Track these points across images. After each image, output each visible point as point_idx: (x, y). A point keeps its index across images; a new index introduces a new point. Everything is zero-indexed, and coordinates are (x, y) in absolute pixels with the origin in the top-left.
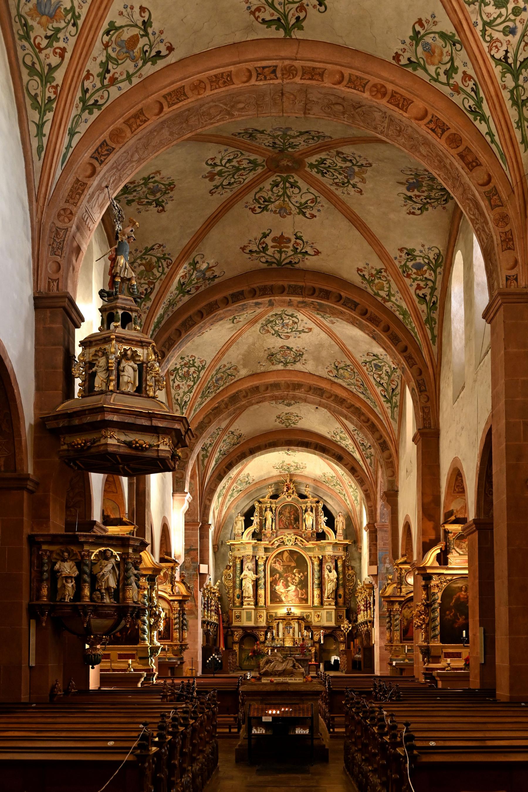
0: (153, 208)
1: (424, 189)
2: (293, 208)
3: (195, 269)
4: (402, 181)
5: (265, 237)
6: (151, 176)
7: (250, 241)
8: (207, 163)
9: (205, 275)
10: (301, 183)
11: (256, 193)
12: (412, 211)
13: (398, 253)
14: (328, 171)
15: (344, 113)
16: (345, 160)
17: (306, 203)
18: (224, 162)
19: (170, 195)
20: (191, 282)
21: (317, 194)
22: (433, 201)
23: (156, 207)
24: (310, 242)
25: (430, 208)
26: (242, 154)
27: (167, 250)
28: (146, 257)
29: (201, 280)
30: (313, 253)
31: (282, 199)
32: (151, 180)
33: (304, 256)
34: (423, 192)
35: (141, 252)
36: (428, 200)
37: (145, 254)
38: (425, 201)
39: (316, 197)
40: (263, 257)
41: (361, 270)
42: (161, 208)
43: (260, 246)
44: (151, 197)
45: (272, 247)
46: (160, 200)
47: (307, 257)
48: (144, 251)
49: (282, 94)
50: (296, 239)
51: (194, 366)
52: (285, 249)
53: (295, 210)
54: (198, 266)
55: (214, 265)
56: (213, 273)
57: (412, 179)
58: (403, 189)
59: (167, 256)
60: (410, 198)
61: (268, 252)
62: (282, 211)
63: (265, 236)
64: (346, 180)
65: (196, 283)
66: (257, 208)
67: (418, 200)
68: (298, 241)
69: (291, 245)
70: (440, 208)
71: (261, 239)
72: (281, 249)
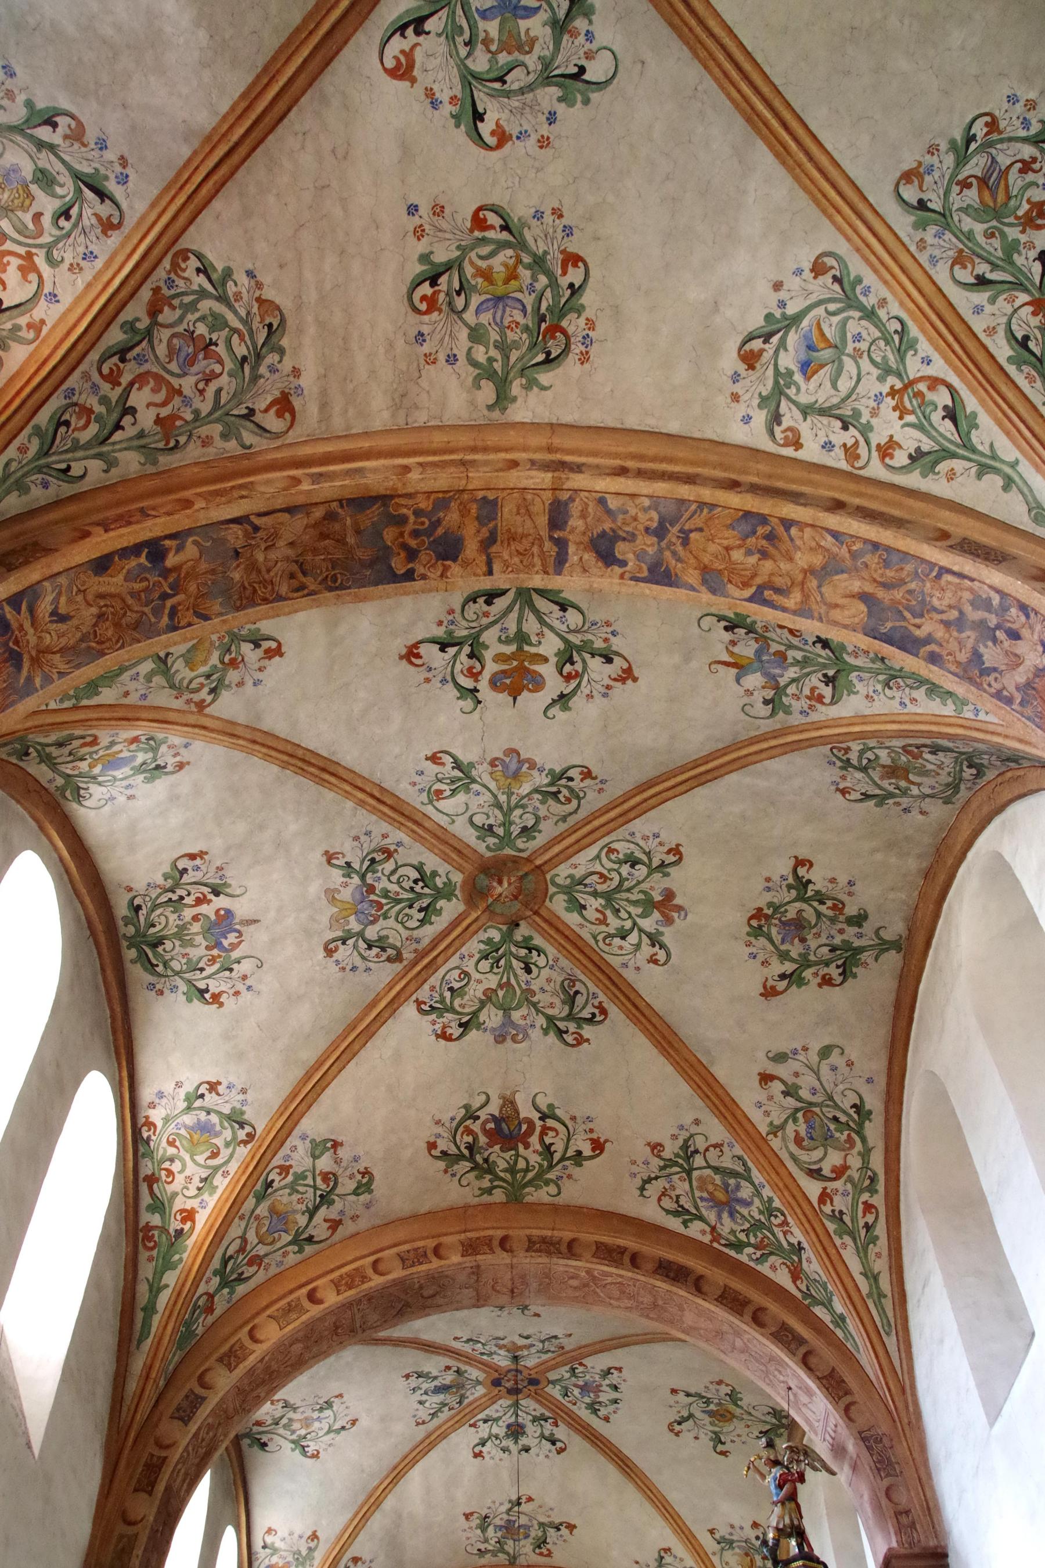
0: (818, 877)
1: (196, 928)
2: (486, 779)
3: (780, 690)
4: (252, 927)
5: (562, 696)
6: (785, 982)
7: (605, 695)
8: (668, 955)
9: (759, 653)
10: (470, 836)
11: (576, 811)
12: (198, 862)
13: (185, 755)
14: (412, 888)
15: (421, 1287)
16: (380, 944)
17: (454, 792)
18: (633, 938)
19: (768, 897)
20: (805, 662)
21: (429, 810)
22: (164, 899)
23: (809, 882)
24: (436, 682)
25: (160, 880)
26: (595, 938)
27: (833, 773)
28: (891, 788)
29: (774, 647)
30: (423, 649)
31: (514, 800)
32: (789, 967)
33: (450, 633)
34: (195, 918)
35: (898, 804)
36: (175, 897)
37: (891, 795)
38: (181, 892)
39: (431, 802)
40: (576, 631)
41: (270, 654)
42: (802, 871)
43: (579, 667)
44: (809, 914)
45: (546, 660)
46: (794, 893)
47: (440, 632)
48: (891, 801)
49: (512, 1292)
52: (510, 649)
53: (482, 772)
54: (770, 694)
55: (720, 667)
56: (733, 643)
57: (234, 946)
58: (241, 908)
59: (839, 764)
60: (217, 893)
61: (556, 644)
62: (513, 766)
63: (563, 700)
64: (370, 878)
65: (791, 647)
66: (577, 777)
67: (197, 891)
68: (467, 683)
69: (491, 668)
70: (140, 886)
71: (574, 692)
72: (520, 649)
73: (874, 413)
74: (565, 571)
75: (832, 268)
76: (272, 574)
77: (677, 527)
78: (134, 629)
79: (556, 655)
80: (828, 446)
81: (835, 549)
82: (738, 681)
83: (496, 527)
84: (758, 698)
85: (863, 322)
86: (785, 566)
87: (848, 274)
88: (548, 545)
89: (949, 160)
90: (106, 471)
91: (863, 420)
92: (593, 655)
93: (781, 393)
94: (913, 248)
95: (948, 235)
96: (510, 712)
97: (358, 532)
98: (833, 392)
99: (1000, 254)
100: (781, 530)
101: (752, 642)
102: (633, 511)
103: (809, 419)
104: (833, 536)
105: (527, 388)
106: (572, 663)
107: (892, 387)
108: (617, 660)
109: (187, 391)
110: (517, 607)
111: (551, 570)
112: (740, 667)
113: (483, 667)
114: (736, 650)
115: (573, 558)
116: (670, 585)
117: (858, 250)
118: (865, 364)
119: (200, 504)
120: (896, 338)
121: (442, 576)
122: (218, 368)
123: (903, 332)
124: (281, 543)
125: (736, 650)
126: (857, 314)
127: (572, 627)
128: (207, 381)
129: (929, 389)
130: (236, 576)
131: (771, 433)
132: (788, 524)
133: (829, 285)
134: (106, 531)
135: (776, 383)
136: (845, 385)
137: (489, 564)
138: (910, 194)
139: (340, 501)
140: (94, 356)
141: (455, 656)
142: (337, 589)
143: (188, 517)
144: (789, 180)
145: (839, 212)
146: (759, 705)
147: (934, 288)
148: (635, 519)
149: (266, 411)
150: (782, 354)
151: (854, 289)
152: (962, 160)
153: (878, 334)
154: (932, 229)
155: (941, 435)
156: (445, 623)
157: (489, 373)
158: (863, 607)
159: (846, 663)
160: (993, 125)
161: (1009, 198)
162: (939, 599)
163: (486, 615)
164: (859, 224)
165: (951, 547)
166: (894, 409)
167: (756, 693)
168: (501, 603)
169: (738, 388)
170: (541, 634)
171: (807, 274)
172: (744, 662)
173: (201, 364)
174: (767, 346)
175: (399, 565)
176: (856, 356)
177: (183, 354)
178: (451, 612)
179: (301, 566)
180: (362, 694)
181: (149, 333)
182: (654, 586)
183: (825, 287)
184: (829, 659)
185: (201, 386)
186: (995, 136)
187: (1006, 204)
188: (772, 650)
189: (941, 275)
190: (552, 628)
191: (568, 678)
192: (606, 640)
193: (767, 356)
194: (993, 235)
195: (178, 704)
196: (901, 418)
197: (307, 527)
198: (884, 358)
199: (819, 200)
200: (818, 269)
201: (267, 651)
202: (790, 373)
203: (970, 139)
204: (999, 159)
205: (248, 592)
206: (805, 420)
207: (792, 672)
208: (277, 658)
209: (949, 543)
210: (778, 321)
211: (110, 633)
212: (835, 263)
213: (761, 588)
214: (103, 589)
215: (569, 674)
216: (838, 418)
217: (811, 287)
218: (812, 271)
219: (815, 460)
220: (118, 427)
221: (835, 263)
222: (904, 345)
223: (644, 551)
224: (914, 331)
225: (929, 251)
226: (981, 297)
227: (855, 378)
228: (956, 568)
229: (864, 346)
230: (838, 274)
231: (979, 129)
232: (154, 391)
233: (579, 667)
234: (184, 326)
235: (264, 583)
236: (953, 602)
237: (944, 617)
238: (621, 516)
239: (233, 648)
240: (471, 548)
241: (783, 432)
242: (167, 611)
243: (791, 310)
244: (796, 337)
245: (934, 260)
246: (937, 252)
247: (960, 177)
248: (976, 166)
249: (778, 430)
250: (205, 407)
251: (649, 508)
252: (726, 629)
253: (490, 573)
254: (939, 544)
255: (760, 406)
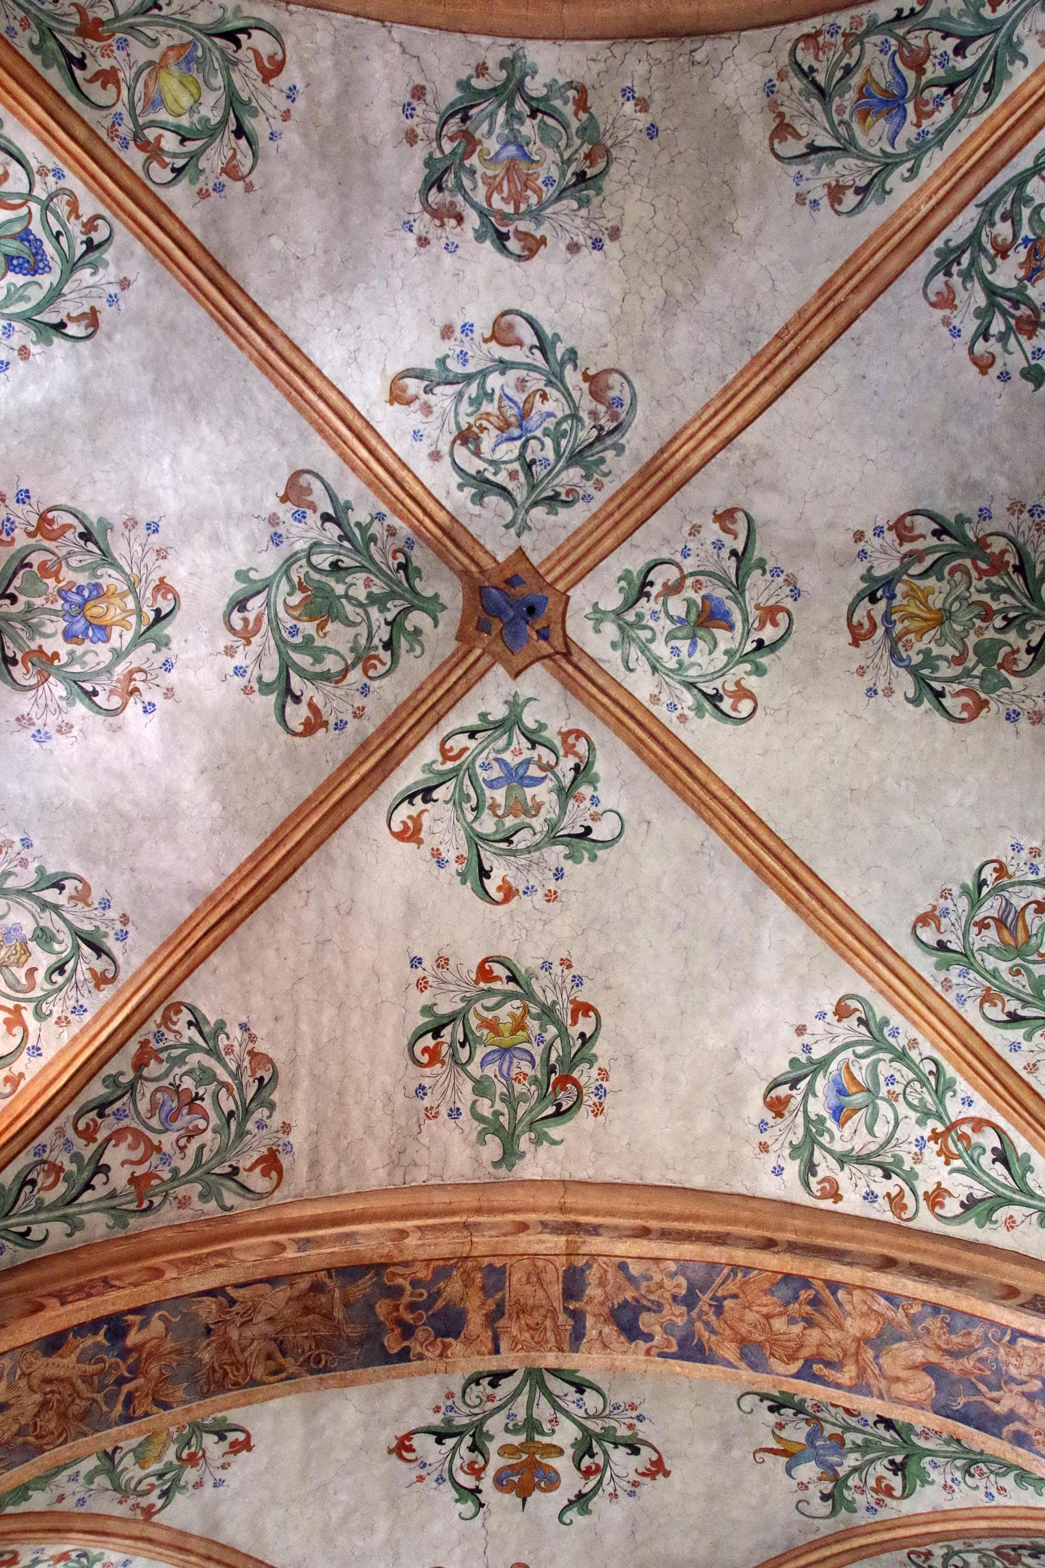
5: (580, 1496)
7: (631, 1494)
9: (811, 1438)
29: (829, 1430)
30: (416, 1441)
33: (448, 1421)
40: (596, 1416)
41: (237, 1448)
43: (599, 1460)
45: (561, 1452)
47: (436, 1420)
50: (478, 1490)
51: (991, 291)
54: (828, 1487)
55: (767, 1456)
56: (781, 1426)
63: (581, 1501)
69: (496, 1462)
71: (594, 1491)
72: (530, 1439)
73: (918, 1159)
74: (582, 1348)
75: (857, 1010)
76: (246, 1354)
77: (709, 1295)
78: (82, 1420)
79: (572, 1446)
80: (870, 1197)
81: (890, 1314)
82: (788, 1471)
83: (503, 1298)
84: (814, 1493)
85: (895, 1064)
86: (834, 1335)
87: (874, 1015)
88: (562, 1318)
89: (964, 903)
90: (69, 1235)
91: (906, 1167)
92: (616, 1445)
93: (814, 1141)
94: (938, 988)
95: (972, 974)
96: (518, 1516)
97: (347, 1305)
98: (870, 1138)
99: (1028, 990)
100: (826, 1293)
101: (803, 1424)
102: (657, 1277)
103: (846, 1167)
104: (887, 1299)
105: (537, 1142)
106: (592, 1455)
107: (933, 1131)
108: (644, 1449)
109: (167, 1148)
110: (527, 1389)
111: (566, 1347)
112: (791, 1456)
113: (486, 1462)
114: (784, 1434)
115: (592, 1333)
116: (704, 1361)
117: (882, 992)
118: (902, 1108)
119: (171, 1274)
120: (932, 1079)
121: (441, 1355)
122: (201, 1124)
123: (938, 1073)
124: (259, 1318)
125: (784, 1434)
126: (888, 1056)
127: (591, 1412)
128: (190, 1138)
129: (973, 1130)
130: (206, 1356)
131: (807, 1185)
132: (834, 1286)
133: (855, 1027)
134: (63, 1304)
135: (807, 1130)
136: (882, 1130)
137: (496, 1340)
138: (928, 935)
139: (328, 1270)
140: (71, 1111)
141: (454, 1449)
142: (319, 1371)
143: (157, 1288)
144: (804, 927)
145: (857, 955)
146: (816, 1501)
147: (966, 1027)
148: (661, 1286)
149: (251, 1169)
150: (811, 1099)
151: (881, 1031)
152: (976, 903)
153: (912, 1076)
154: (955, 970)
155: (994, 1180)
156: (443, 1409)
157: (497, 1129)
158: (929, 1380)
159: (914, 1445)
160: (1001, 870)
161: (1029, 937)
162: (1017, 1367)
163: (491, 1398)
164: (880, 967)
165: (1022, 1305)
166: (939, 1154)
167: (811, 1486)
168: (508, 1386)
169: (765, 1138)
170: (554, 1421)
171: (831, 1018)
172: (795, 1449)
173: (185, 1119)
174: (794, 1092)
175: (392, 1343)
176: (892, 1099)
177: (166, 1109)
178: (450, 1395)
179: (281, 1345)
180: (343, 1497)
181: (132, 1087)
182: (686, 1363)
183: (851, 1029)
184: (895, 1442)
185: (182, 1142)
186: (1005, 880)
187: (1027, 942)
188: (826, 1434)
189: (971, 1012)
190: (567, 1414)
191: (587, 1473)
192: (631, 1427)
193: (795, 1102)
194: (1018, 973)
195: (121, 1510)
196: (947, 1163)
197: (290, 1299)
198: (921, 1100)
199: (836, 944)
200: (842, 1012)
201: (232, 1445)
202: (821, 1120)
203: (981, 884)
204: (1014, 900)
205: (218, 1375)
206: (842, 1169)
207: (852, 1460)
208: (244, 1453)
209: (1020, 1300)
210: (804, 1066)
211: (52, 1425)
212: (859, 1006)
213: (809, 1362)
214: (51, 1372)
215: (589, 1468)
216: (879, 1165)
217: (835, 1030)
218: (835, 1014)
219: (858, 1213)
220: (88, 1186)
221: (859, 1006)
222: (942, 1087)
223: (672, 1324)
224: (950, 1071)
225: (956, 990)
226: (1016, 1034)
227: (892, 1122)
228: (1031, 1330)
229: (898, 1088)
230: (863, 1016)
231: (988, 874)
232: (131, 1147)
233: (599, 1460)
234: (170, 1079)
235: (236, 1364)
236: (1033, 1370)
237: (1025, 1388)
238: (644, 1284)
239: (194, 1441)
240: (475, 1322)
241: (819, 1183)
242: (122, 1398)
243: (817, 1054)
244: (825, 1082)
245: (961, 999)
246: (964, 992)
247: (977, 919)
248: (991, 908)
249: (813, 1181)
250: (185, 1166)
251: (676, 1273)
252: (771, 1409)
253: (497, 1351)
254: (1008, 1302)
255: (792, 1157)
